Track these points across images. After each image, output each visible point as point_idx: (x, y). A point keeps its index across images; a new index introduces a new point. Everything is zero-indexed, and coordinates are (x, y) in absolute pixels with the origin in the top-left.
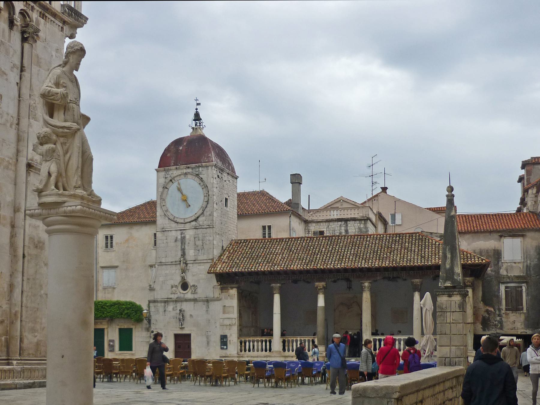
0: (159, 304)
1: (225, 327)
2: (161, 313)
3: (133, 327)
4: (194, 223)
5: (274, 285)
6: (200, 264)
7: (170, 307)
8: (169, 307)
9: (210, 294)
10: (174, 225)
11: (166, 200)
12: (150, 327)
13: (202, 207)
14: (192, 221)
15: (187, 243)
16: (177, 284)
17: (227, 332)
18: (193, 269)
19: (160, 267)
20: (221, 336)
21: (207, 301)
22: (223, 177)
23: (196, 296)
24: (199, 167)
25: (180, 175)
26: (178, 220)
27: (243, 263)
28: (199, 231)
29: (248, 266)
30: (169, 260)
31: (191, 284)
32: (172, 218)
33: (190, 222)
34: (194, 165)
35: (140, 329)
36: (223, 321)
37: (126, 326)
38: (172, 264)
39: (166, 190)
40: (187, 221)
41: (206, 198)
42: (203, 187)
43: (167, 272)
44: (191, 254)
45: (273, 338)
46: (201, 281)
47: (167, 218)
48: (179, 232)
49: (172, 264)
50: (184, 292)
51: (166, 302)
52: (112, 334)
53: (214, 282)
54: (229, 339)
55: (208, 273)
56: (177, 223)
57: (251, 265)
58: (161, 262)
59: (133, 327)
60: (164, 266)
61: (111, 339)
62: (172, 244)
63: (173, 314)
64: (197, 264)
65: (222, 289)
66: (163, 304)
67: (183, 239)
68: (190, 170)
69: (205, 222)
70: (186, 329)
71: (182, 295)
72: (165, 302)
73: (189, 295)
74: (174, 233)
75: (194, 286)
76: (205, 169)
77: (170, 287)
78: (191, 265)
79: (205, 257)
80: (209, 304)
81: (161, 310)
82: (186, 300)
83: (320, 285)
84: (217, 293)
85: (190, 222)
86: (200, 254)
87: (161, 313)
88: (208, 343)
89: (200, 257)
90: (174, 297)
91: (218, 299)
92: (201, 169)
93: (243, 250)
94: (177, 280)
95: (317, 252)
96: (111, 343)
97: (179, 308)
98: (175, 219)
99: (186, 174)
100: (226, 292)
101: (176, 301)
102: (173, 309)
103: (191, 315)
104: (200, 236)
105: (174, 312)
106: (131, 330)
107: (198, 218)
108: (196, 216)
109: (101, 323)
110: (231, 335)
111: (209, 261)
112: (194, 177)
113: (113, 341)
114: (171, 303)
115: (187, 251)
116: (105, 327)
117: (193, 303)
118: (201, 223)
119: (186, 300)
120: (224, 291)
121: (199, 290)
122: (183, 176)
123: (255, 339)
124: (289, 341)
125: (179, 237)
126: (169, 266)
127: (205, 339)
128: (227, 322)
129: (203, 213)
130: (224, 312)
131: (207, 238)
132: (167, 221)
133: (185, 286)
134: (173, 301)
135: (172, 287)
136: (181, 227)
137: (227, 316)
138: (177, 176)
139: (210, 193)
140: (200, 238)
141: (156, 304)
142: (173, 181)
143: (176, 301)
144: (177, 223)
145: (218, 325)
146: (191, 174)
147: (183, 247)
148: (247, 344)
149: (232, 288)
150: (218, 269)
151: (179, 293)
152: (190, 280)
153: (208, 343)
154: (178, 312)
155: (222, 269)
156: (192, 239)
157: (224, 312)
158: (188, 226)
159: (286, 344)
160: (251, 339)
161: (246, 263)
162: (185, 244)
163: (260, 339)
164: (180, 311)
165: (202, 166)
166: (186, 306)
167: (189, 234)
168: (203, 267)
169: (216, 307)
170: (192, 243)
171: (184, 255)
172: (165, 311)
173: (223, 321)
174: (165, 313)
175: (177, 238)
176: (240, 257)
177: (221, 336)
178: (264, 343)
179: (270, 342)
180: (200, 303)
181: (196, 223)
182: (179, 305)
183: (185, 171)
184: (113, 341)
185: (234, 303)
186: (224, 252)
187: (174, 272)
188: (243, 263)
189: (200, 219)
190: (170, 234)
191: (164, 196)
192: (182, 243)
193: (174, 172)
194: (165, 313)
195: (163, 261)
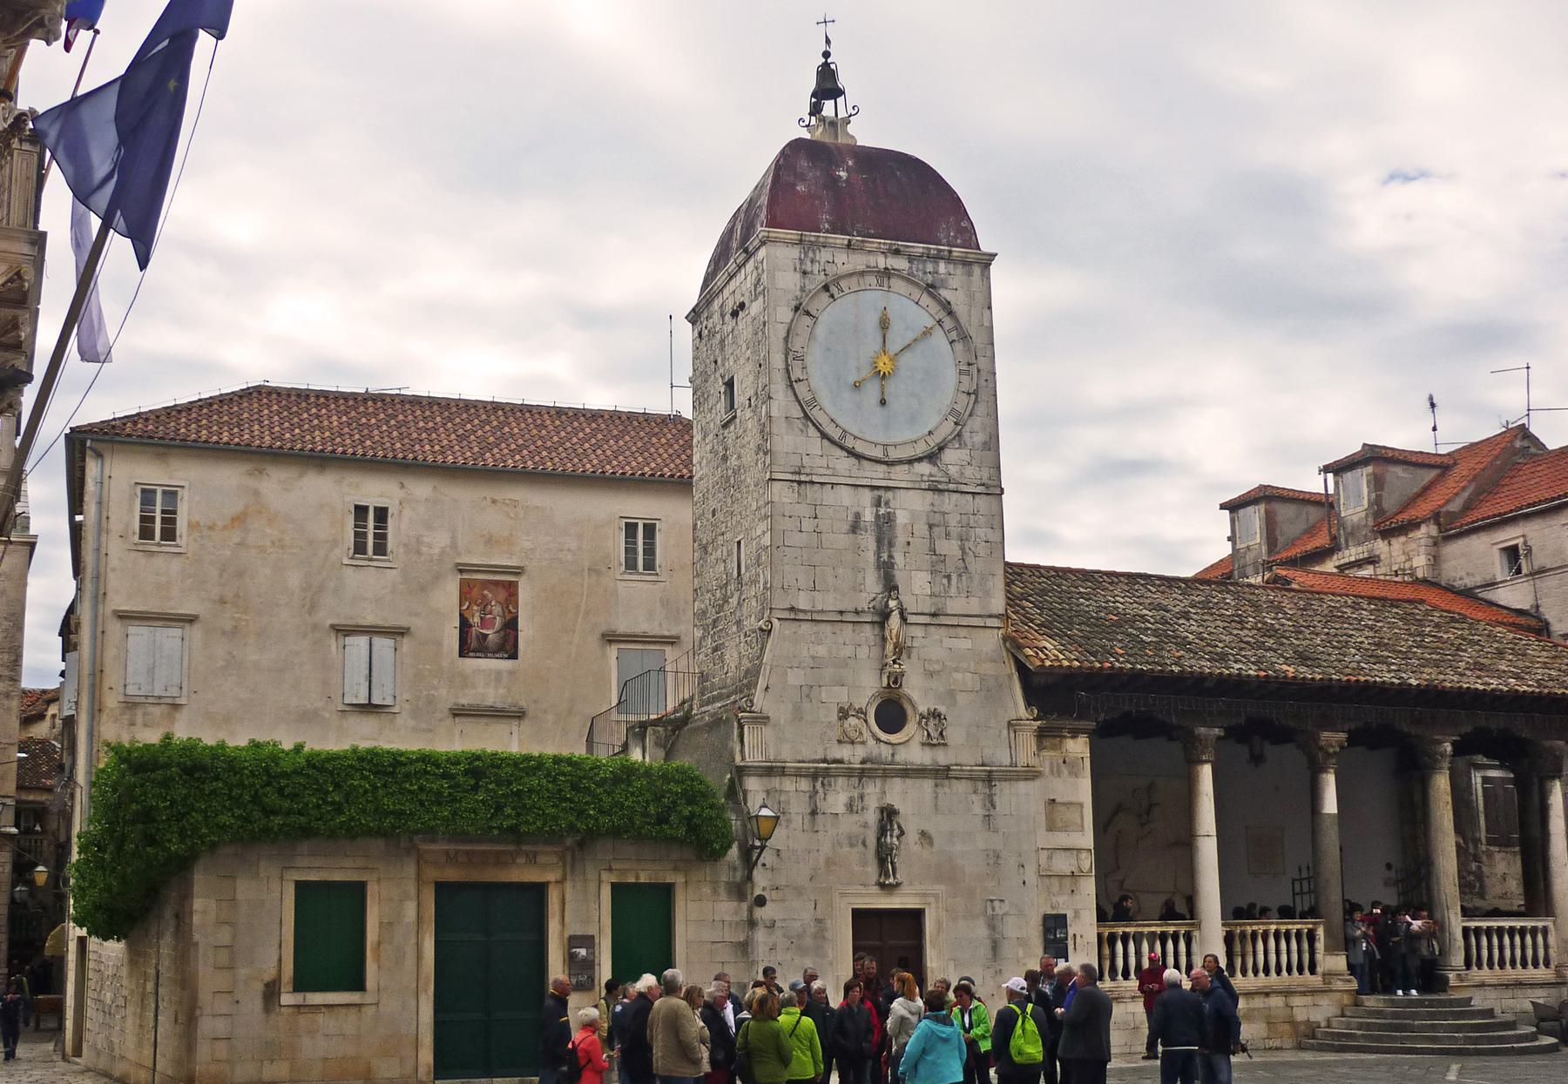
0: (788, 784)
1: (1055, 881)
2: (797, 821)
3: (678, 879)
4: (924, 468)
5: (1203, 730)
6: (952, 631)
7: (837, 798)
8: (830, 798)
9: (1001, 757)
10: (844, 464)
11: (809, 360)
12: (749, 878)
14: (920, 460)
15: (901, 539)
16: (860, 702)
17: (1063, 905)
18: (930, 645)
19: (789, 629)
20: (1046, 918)
21: (988, 778)
23: (943, 757)
24: (937, 258)
25: (862, 273)
26: (860, 448)
28: (949, 502)
30: (829, 602)
31: (923, 709)
32: (835, 434)
33: (910, 462)
34: (919, 248)
35: (706, 890)
36: (1050, 858)
38: (841, 618)
39: (807, 320)
40: (894, 454)
41: (965, 379)
42: (954, 335)
43: (821, 651)
44: (916, 586)
45: (1199, 926)
46: (962, 699)
47: (812, 430)
48: (867, 497)
49: (841, 618)
50: (893, 738)
51: (821, 774)
52: (580, 914)
53: (1017, 706)
54: (1071, 932)
56: (859, 457)
58: (792, 609)
59: (678, 879)
60: (805, 626)
61: (578, 930)
62: (843, 540)
63: (849, 824)
64: (942, 631)
65: (1041, 735)
66: (804, 785)
67: (885, 524)
68: (901, 264)
69: (969, 472)
70: (905, 889)
71: (885, 752)
72: (814, 776)
73: (910, 747)
74: (845, 496)
75: (936, 715)
76: (959, 270)
77: (834, 716)
78: (918, 632)
79: (974, 606)
80: (996, 790)
81: (798, 808)
82: (907, 772)
84: (1027, 750)
85: (910, 462)
86: (953, 591)
87: (797, 821)
88: (995, 947)
89: (955, 605)
90: (853, 755)
91: (1031, 775)
92: (942, 267)
94: (867, 689)
96: (583, 952)
97: (873, 803)
98: (849, 443)
99: (887, 273)
101: (867, 772)
102: (850, 807)
104: (953, 520)
105: (855, 817)
106: (667, 891)
107: (941, 449)
108: (933, 441)
109: (532, 859)
110: (1077, 914)
112: (916, 293)
113: (588, 941)
114: (840, 780)
115: (900, 577)
116: (551, 876)
117: (927, 785)
118: (953, 471)
119: (907, 772)
120: (1047, 742)
121: (955, 735)
122: (872, 280)
123: (1146, 930)
124: (1243, 935)
125: (868, 516)
126: (827, 629)
127: (982, 931)
128: (1063, 864)
130: (1051, 827)
131: (980, 532)
132: (815, 444)
133: (891, 714)
134: (849, 773)
135: (844, 714)
136: (876, 474)
137: (1062, 839)
138: (851, 275)
140: (954, 531)
141: (776, 782)
142: (834, 290)
143: (867, 772)
144: (859, 457)
145: (1030, 874)
146: (908, 279)
147: (885, 556)
148: (1119, 946)
149: (1075, 734)
151: (871, 742)
152: (918, 693)
153: (995, 947)
154: (872, 817)
156: (921, 528)
157: (1051, 827)
158: (900, 475)
159: (1238, 948)
160: (1260, 929)
162: (891, 545)
164: (888, 815)
165: (949, 259)
166: (904, 796)
167: (909, 508)
168: (967, 644)
169: (1020, 799)
170: (920, 544)
171: (890, 587)
172: (814, 813)
173: (1050, 858)
174: (813, 821)
175: (858, 516)
177: (1046, 918)
180: (961, 787)
181: (934, 470)
182: (872, 789)
183: (882, 262)
184: (588, 941)
185: (1083, 790)
187: (848, 651)
189: (949, 456)
190: (828, 496)
191: (797, 344)
192: (879, 541)
194: (813, 821)
195: (803, 602)
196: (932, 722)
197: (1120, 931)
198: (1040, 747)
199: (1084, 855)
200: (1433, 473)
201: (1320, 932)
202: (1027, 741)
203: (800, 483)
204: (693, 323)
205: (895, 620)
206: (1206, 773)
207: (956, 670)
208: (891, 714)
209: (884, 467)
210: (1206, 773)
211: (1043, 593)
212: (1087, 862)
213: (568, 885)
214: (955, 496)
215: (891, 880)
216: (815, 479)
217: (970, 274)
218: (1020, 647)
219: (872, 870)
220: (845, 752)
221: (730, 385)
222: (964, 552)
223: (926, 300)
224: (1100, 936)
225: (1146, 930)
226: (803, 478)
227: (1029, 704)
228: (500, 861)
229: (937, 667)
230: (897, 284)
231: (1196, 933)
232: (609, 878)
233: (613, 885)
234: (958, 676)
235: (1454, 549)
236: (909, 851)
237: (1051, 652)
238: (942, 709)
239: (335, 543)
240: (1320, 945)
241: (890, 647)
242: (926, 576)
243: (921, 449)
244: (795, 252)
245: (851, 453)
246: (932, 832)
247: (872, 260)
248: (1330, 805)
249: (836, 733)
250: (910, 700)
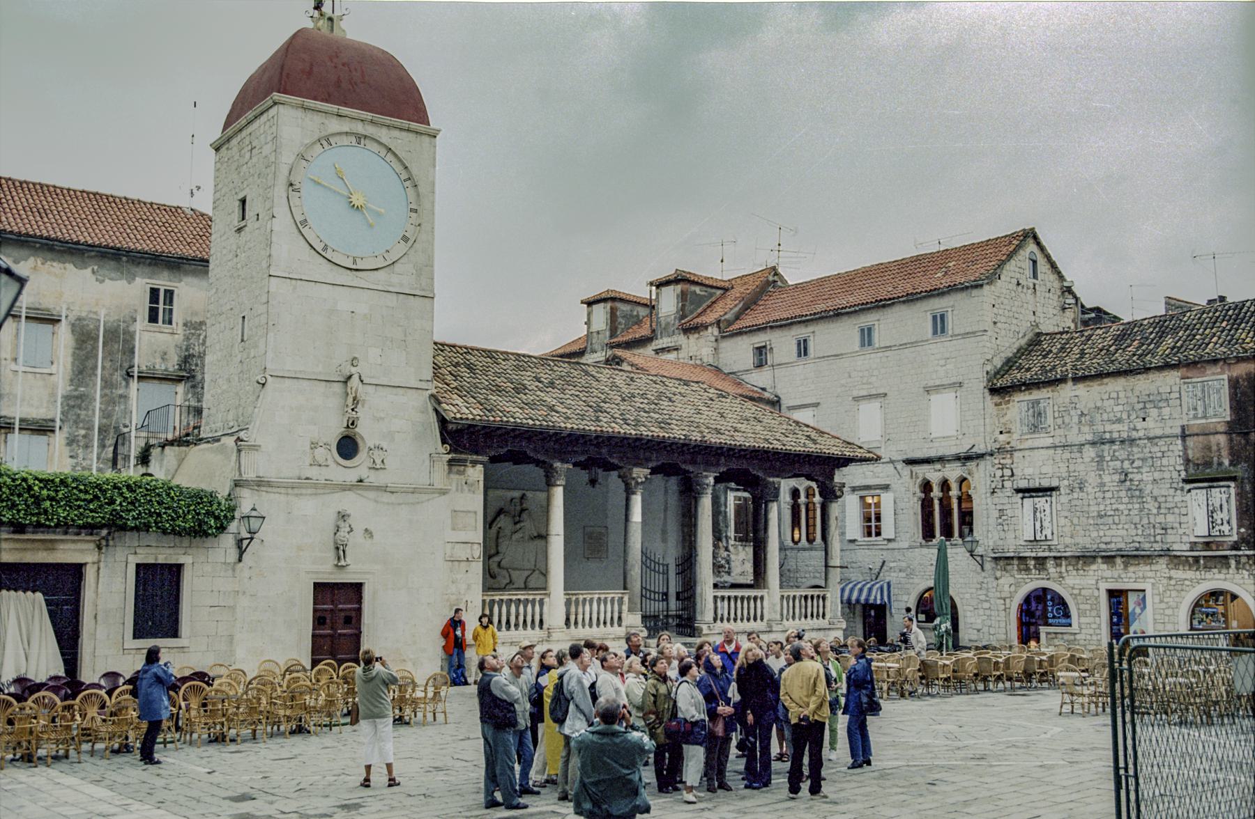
9: (423, 480)
37: (161, 553)
65: (451, 463)
78: (370, 389)
83: (640, 473)
91: (443, 492)
100: (459, 473)
103: (366, 530)
120: (455, 469)
128: (462, 552)
133: (348, 447)
135: (314, 445)
148: (496, 609)
149: (474, 463)
151: (332, 465)
152: (367, 432)
159: (573, 609)
163: (522, 598)
169: (437, 509)
178: (529, 607)
179: (541, 603)
183: (360, 128)
196: (376, 452)
197: (497, 598)
198: (450, 472)
199: (476, 546)
200: (719, 292)
201: (626, 599)
202: (442, 466)
204: (217, 150)
205: (355, 381)
206: (558, 494)
208: (348, 447)
210: (558, 494)
211: (455, 363)
212: (478, 551)
213: (102, 565)
215: (342, 563)
218: (439, 403)
219: (331, 555)
220: (314, 472)
221: (243, 201)
224: (484, 601)
225: (514, 598)
227: (444, 442)
228: (50, 545)
231: (546, 600)
232: (133, 561)
233: (138, 565)
235: (726, 345)
236: (356, 542)
237: (462, 409)
238: (384, 445)
240: (625, 608)
241: (350, 400)
246: (371, 528)
248: (637, 515)
249: (308, 461)
250: (362, 438)
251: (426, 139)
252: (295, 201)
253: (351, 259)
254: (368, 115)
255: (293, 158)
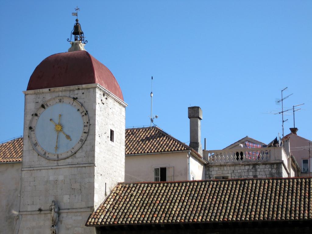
4: (69, 160)
10: (44, 162)
13: (81, 140)
14: (68, 158)
22: (109, 103)
26: (51, 156)
27: (132, 214)
29: (139, 216)
39: (36, 118)
40: (60, 157)
41: (86, 128)
44: (66, 200)
55: (86, 225)
57: (143, 216)
74: (44, 172)
85: (65, 159)
92: (80, 92)
93: (132, 195)
95: (227, 199)
108: (73, 151)
111: (87, 210)
129: (81, 147)
139: (91, 122)
150: (100, 220)
155: (105, 220)
158: (61, 163)
161: (136, 213)
165: (82, 89)
176: (129, 205)
186: (108, 198)
188: (132, 214)
189: (77, 155)
193: (46, 94)
203: (30, 170)
207: (76, 227)
209: (56, 162)
214: (79, 168)
216: (35, 169)
217: (89, 92)
222: (80, 186)
223: (75, 103)
226: (31, 169)
229: (70, 226)
230: (66, 100)
234: (76, 229)
239: (16, 190)
242: (68, 196)
243: (70, 154)
244: (33, 96)
245: (48, 159)
247: (57, 94)
251: (92, 90)
252: (33, 135)
253: (55, 157)
254: (64, 88)
255: (31, 117)
